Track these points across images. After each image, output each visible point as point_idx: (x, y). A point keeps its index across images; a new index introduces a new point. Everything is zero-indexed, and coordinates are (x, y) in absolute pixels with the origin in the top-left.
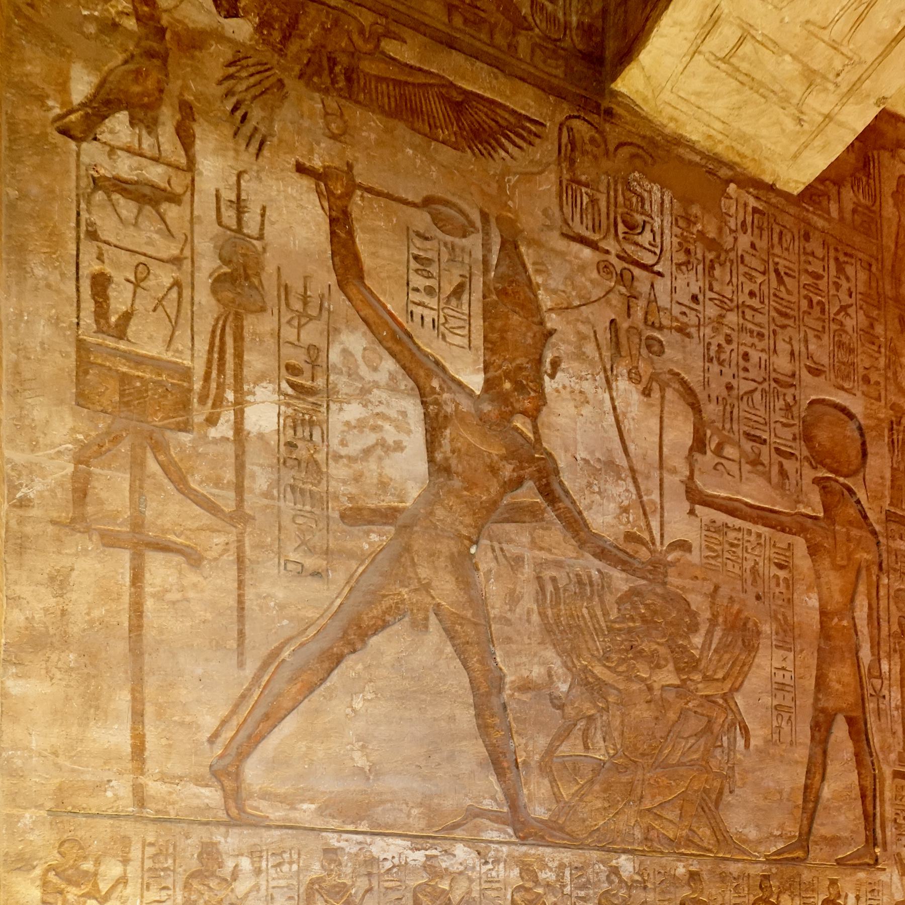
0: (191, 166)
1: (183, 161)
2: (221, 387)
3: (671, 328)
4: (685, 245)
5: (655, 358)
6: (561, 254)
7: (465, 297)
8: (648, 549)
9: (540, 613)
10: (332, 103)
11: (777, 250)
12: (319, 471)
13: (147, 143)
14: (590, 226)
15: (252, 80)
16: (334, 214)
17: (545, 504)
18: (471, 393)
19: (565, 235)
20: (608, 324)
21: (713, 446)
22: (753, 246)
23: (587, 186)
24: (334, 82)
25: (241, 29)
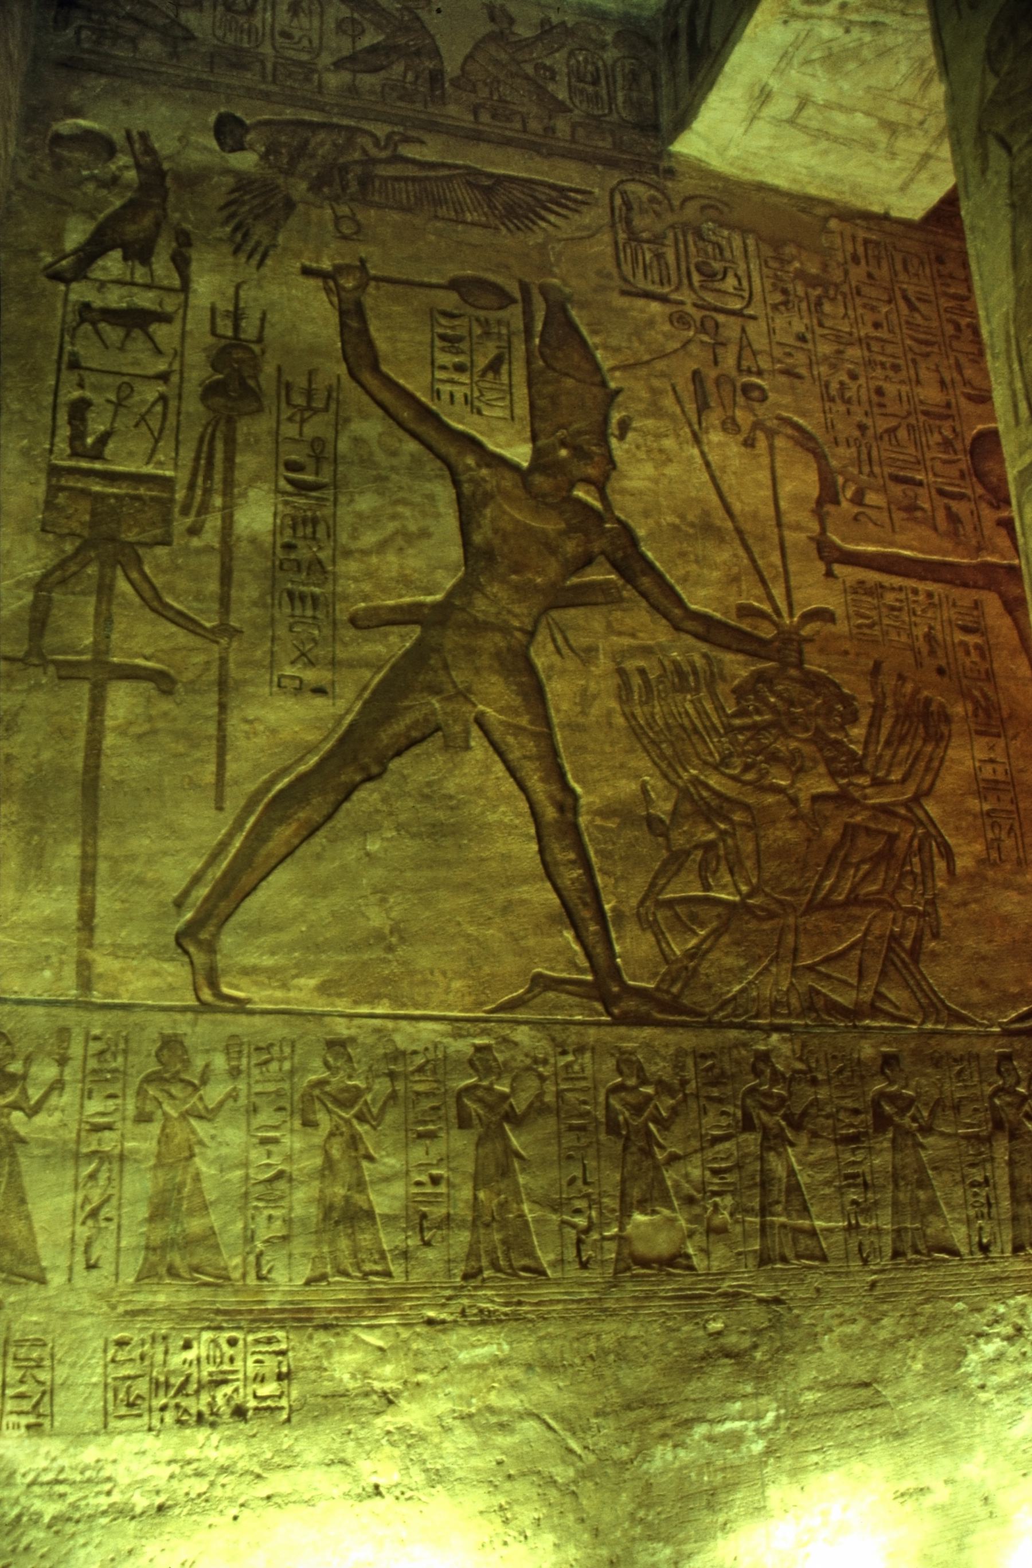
0: (185, 287)
1: (177, 283)
2: (207, 492)
3: (773, 372)
4: (780, 285)
5: (756, 405)
6: (622, 312)
7: (505, 368)
8: (774, 623)
9: (624, 714)
10: (344, 210)
11: (902, 277)
12: (324, 571)
13: (140, 274)
14: (657, 279)
15: (255, 202)
16: (345, 307)
17: (621, 582)
18: (514, 467)
19: (624, 293)
20: (689, 375)
21: (849, 494)
22: (870, 276)
23: (648, 241)
24: (344, 188)
25: (246, 161)
